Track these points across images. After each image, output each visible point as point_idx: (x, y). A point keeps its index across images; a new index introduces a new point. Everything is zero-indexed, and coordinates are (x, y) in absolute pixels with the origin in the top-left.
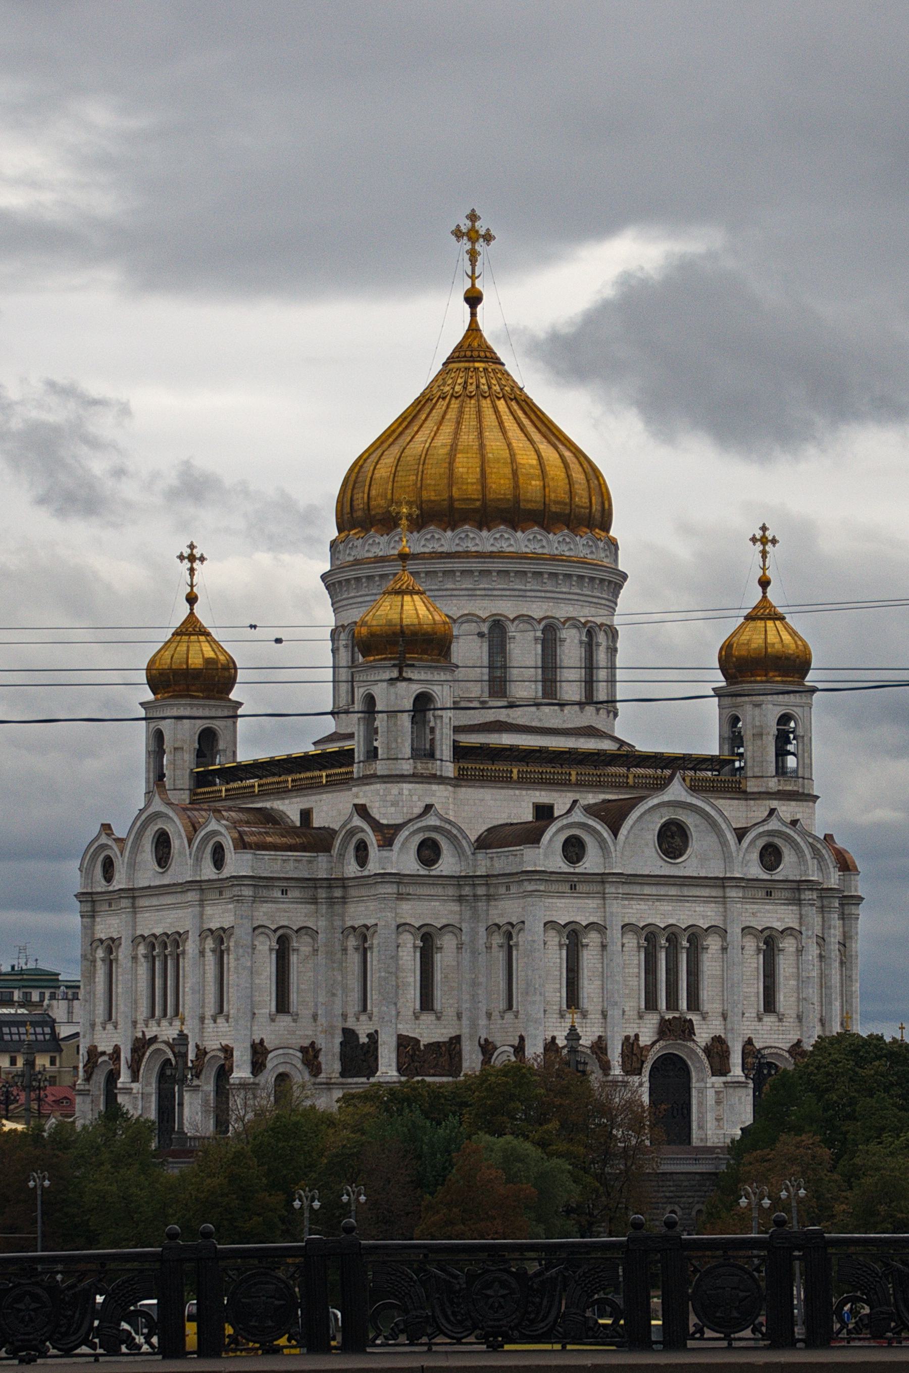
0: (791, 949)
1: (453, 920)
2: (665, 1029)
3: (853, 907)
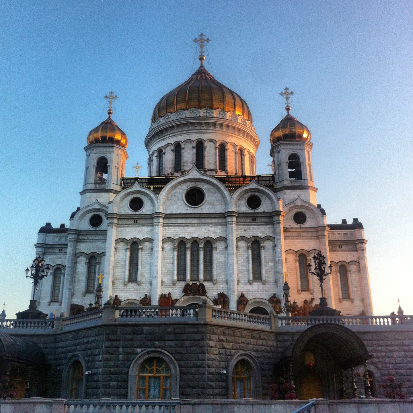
2: (187, 290)
3: (360, 245)
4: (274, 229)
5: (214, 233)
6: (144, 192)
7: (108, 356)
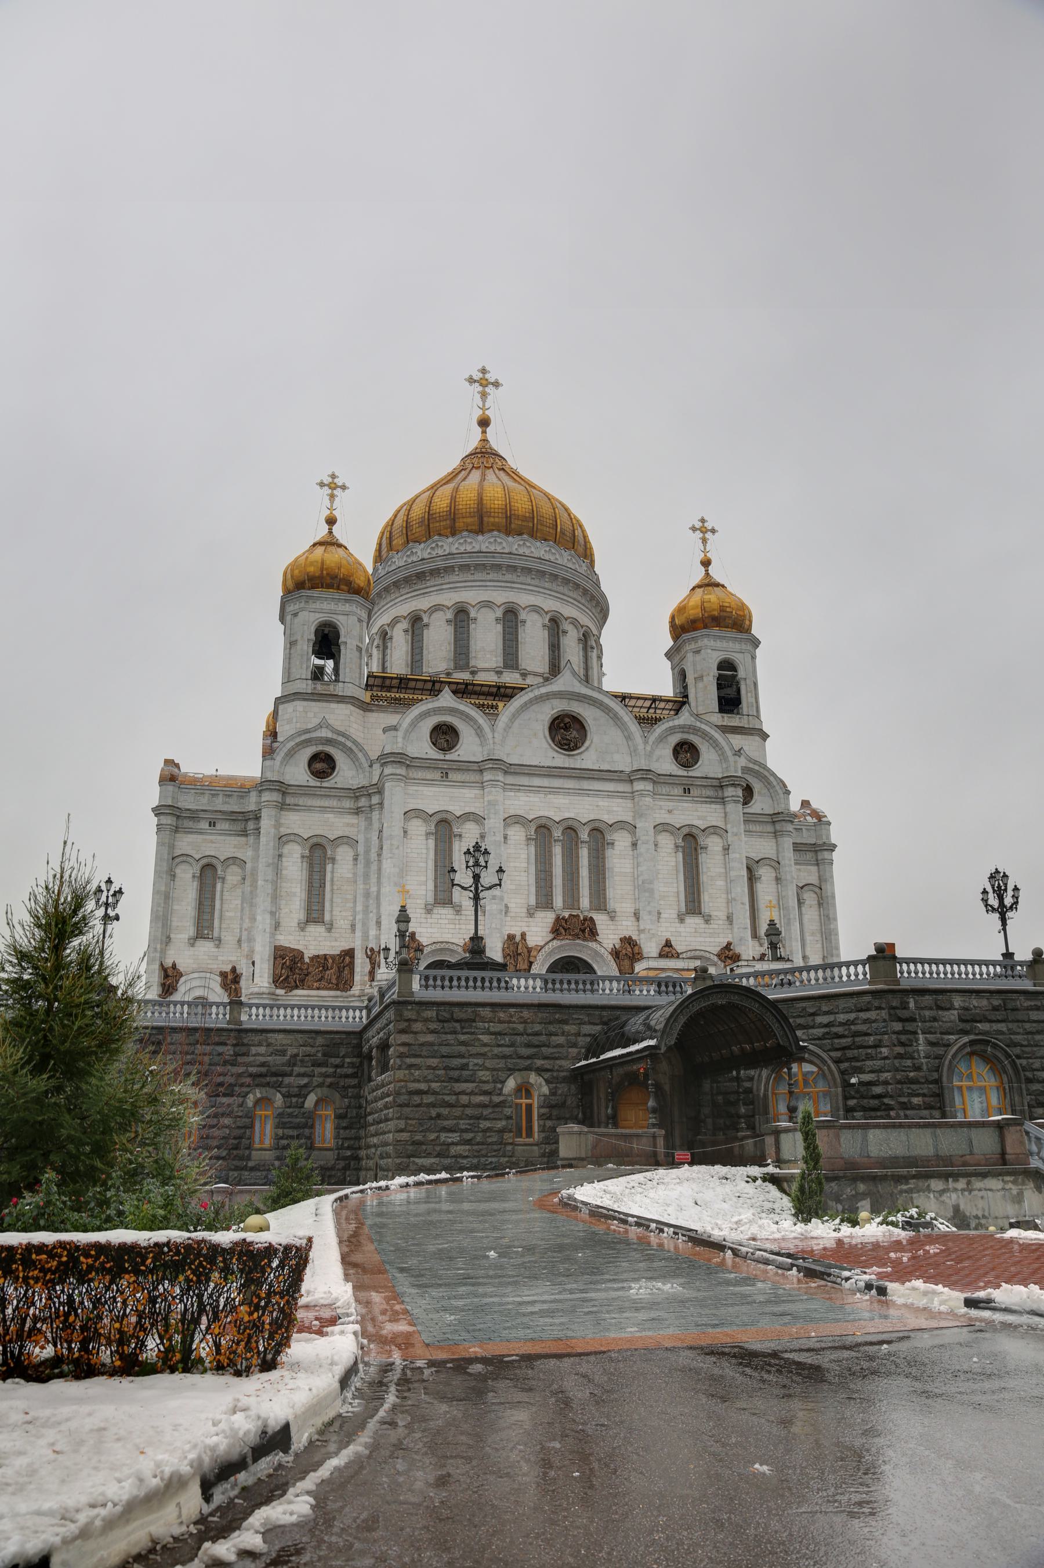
0: (716, 848)
2: (560, 928)
3: (826, 853)
4: (725, 813)
5: (609, 812)
6: (462, 713)
7: (900, 1050)
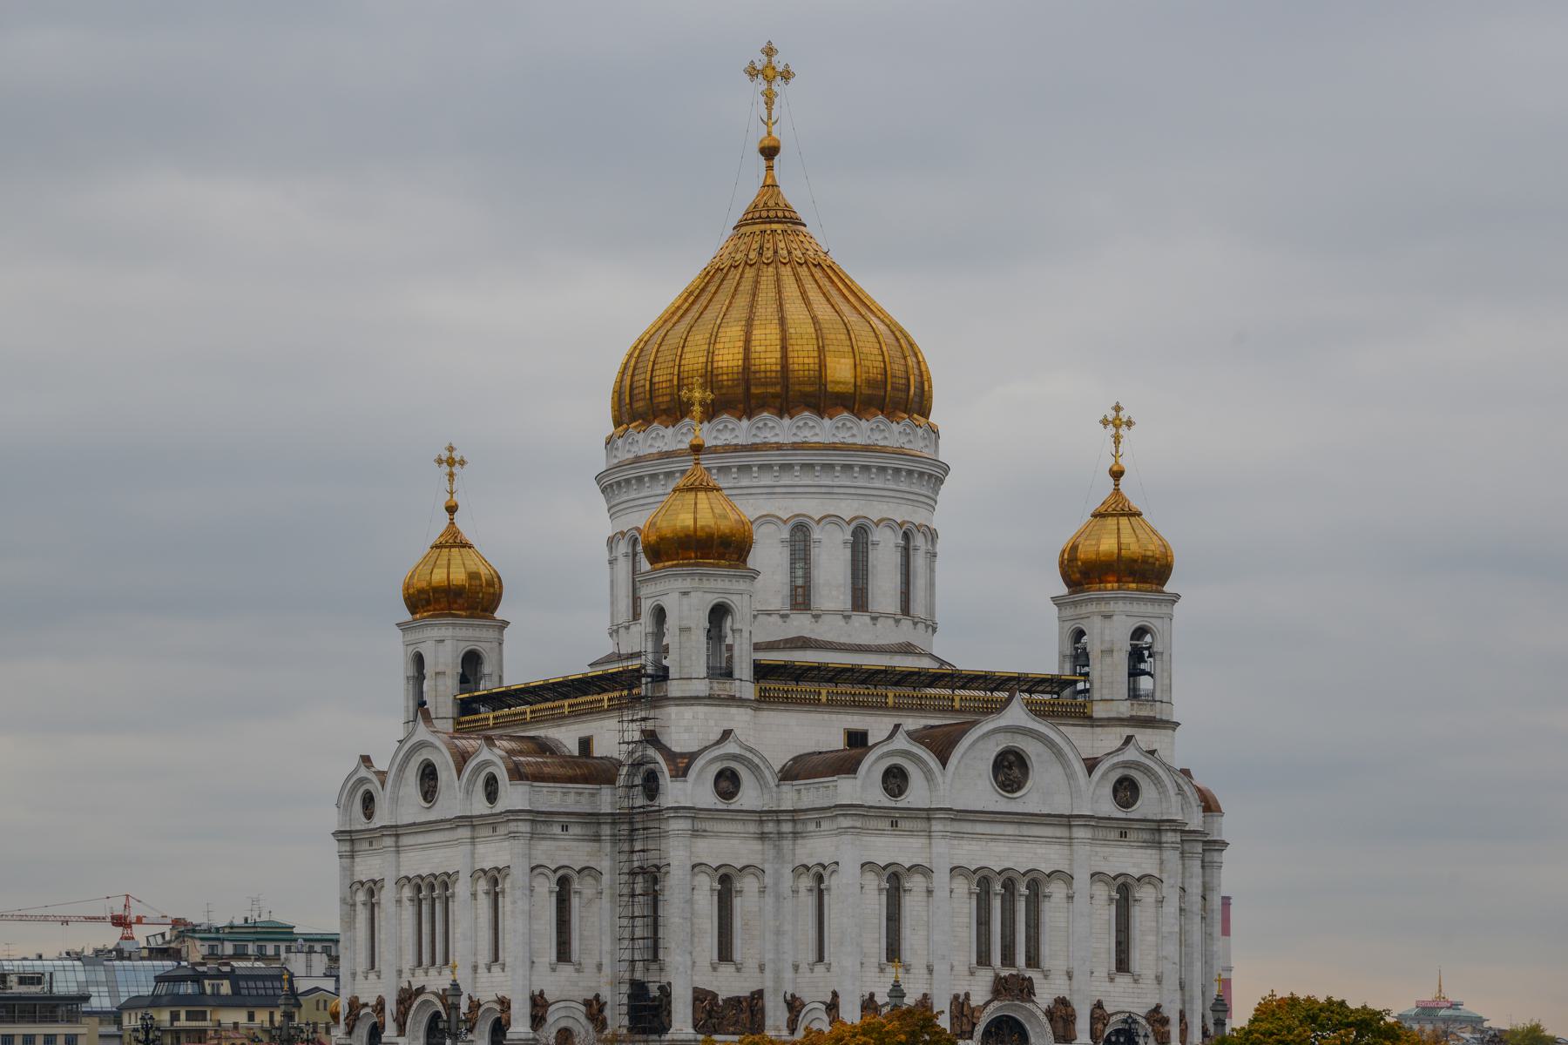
1: (755, 860)
2: (1002, 988)
